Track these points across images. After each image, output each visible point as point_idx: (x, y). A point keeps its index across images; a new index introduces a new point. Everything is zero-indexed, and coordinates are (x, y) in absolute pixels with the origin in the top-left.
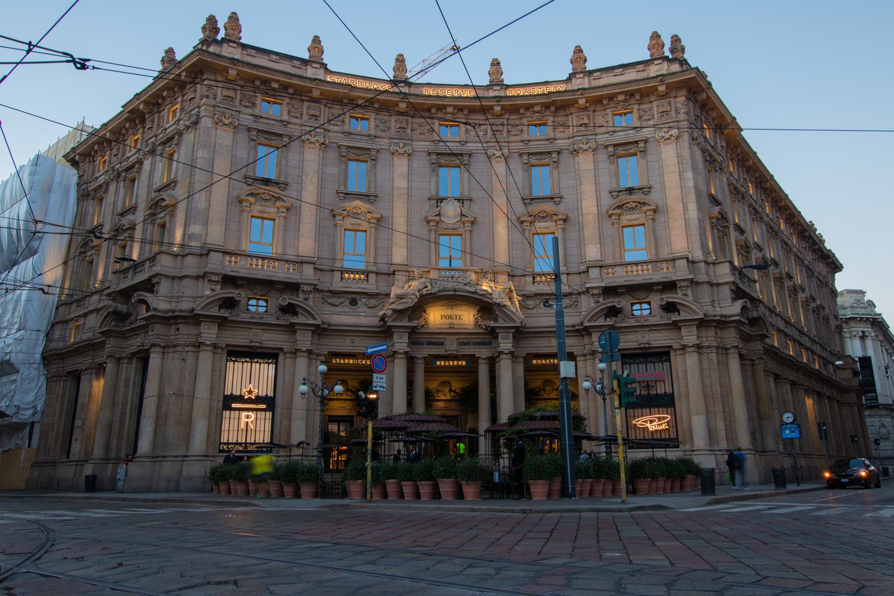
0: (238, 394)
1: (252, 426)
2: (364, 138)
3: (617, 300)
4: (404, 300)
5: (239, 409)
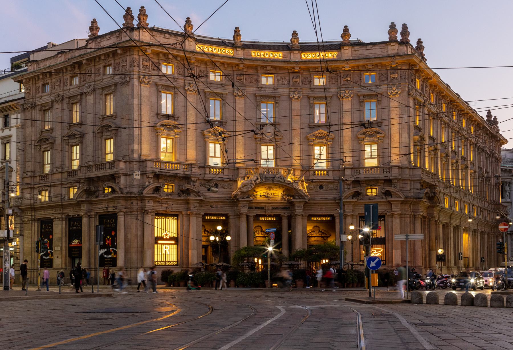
0: (160, 236)
1: (168, 253)
2: (219, 86)
3: (359, 188)
4: (247, 187)
5: (162, 244)
